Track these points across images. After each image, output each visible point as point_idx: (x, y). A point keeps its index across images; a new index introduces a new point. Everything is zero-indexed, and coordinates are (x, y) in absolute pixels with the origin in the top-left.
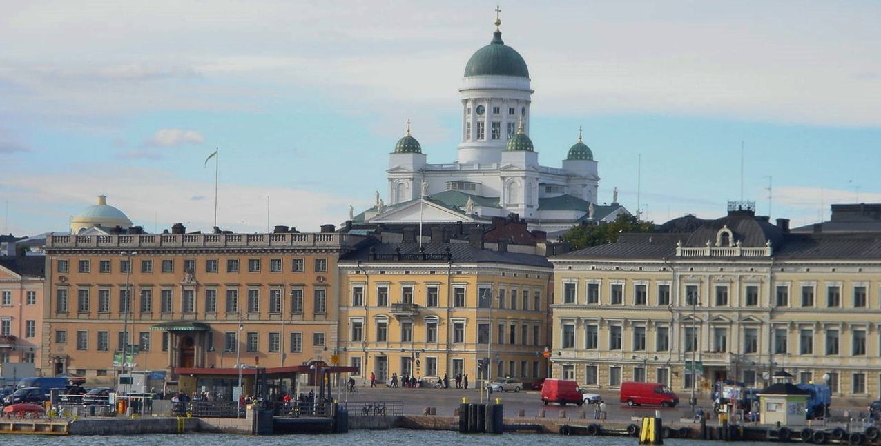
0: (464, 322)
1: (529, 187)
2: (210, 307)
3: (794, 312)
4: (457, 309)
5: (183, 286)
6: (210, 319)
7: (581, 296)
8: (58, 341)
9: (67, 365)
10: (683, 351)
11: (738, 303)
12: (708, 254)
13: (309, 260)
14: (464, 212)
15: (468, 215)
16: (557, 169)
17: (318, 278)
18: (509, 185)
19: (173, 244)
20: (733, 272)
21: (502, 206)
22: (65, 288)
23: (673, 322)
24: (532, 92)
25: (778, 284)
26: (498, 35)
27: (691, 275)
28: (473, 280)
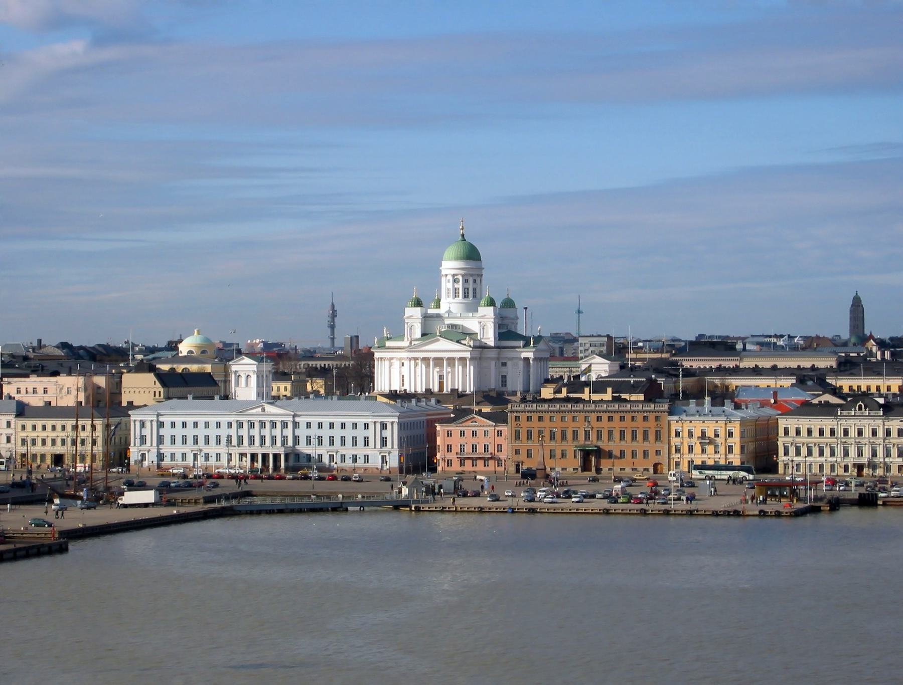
0: (733, 445)
4: (729, 439)
5: (584, 428)
6: (600, 444)
7: (792, 432)
8: (516, 454)
10: (842, 456)
12: (853, 414)
15: (467, 346)
17: (657, 425)
18: (483, 328)
20: (866, 422)
21: (479, 339)
24: (483, 269)
25: (886, 427)
26: (463, 235)
27: (845, 423)
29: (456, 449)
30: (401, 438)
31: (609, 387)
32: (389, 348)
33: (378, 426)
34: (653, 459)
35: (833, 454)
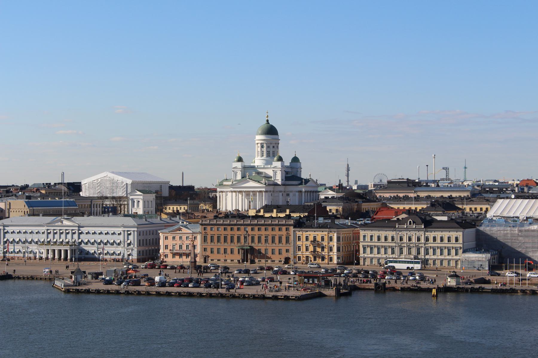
0: (333, 246)
1: (282, 173)
2: (253, 241)
3: (431, 243)
5: (244, 235)
6: (253, 245)
7: (368, 239)
8: (205, 250)
9: (208, 258)
10: (399, 254)
11: (414, 241)
12: (406, 227)
13: (284, 228)
14: (262, 183)
16: (287, 166)
17: (287, 233)
18: (275, 173)
19: (240, 223)
20: (413, 233)
22: (206, 235)
23: (396, 246)
24: (280, 140)
25: (426, 236)
28: (335, 234)
29: (170, 247)
30: (140, 240)
31: (287, 209)
32: (225, 185)
33: (126, 232)
34: (285, 255)
35: (393, 253)
